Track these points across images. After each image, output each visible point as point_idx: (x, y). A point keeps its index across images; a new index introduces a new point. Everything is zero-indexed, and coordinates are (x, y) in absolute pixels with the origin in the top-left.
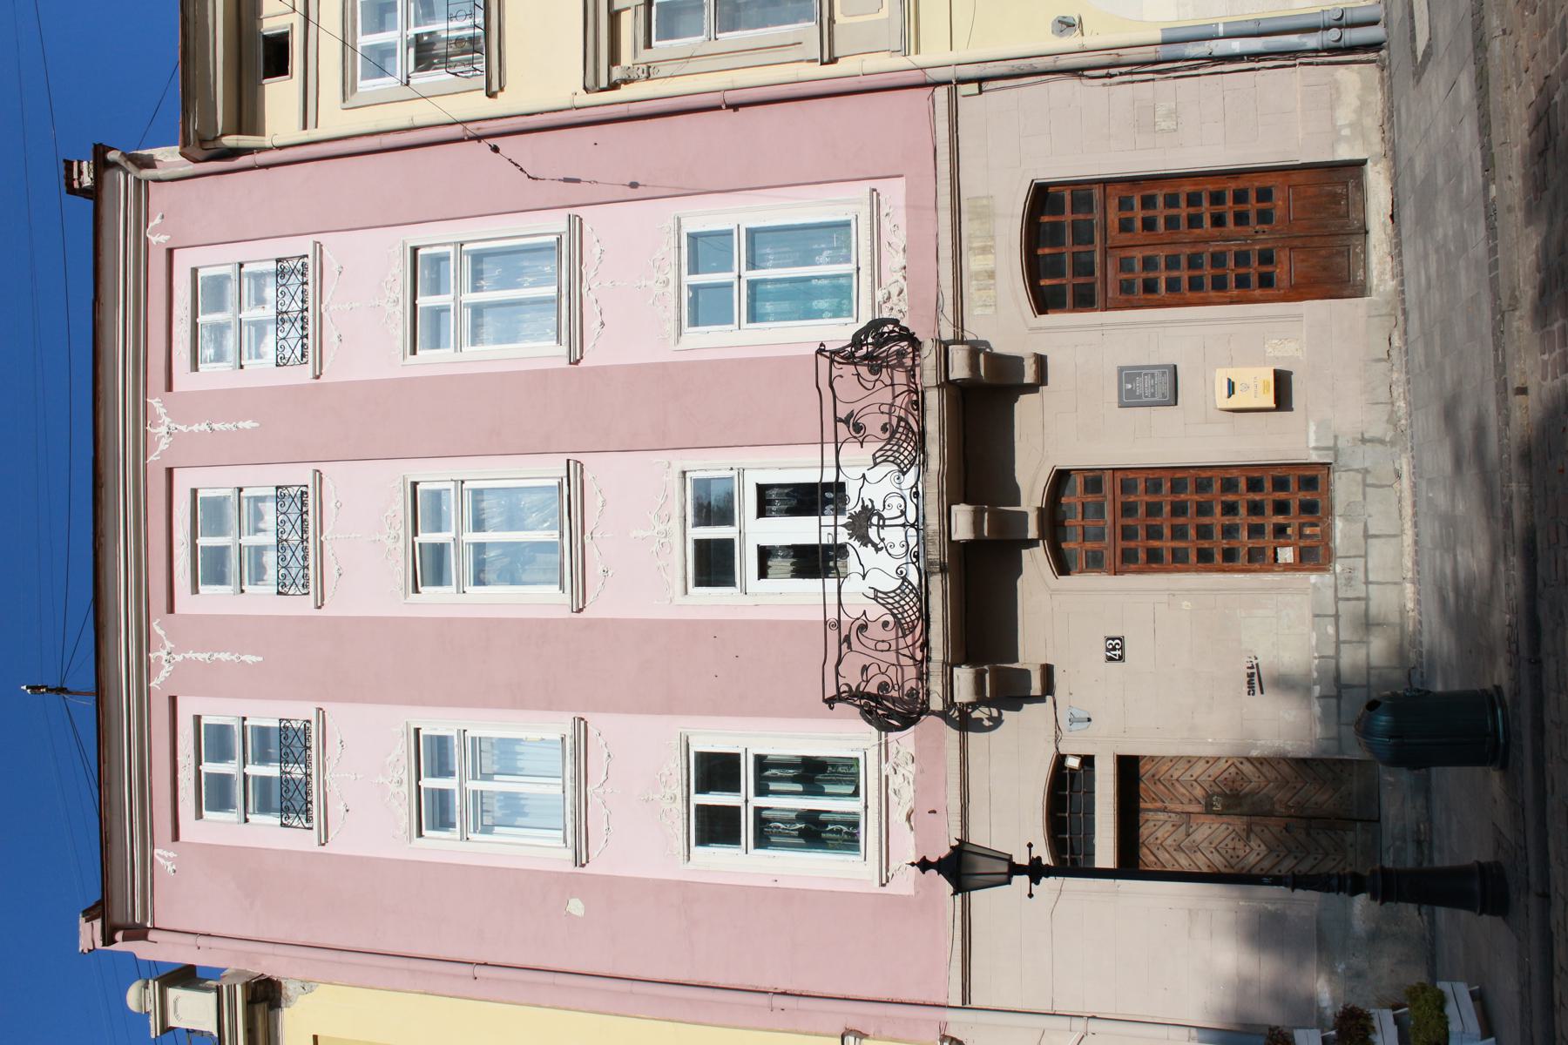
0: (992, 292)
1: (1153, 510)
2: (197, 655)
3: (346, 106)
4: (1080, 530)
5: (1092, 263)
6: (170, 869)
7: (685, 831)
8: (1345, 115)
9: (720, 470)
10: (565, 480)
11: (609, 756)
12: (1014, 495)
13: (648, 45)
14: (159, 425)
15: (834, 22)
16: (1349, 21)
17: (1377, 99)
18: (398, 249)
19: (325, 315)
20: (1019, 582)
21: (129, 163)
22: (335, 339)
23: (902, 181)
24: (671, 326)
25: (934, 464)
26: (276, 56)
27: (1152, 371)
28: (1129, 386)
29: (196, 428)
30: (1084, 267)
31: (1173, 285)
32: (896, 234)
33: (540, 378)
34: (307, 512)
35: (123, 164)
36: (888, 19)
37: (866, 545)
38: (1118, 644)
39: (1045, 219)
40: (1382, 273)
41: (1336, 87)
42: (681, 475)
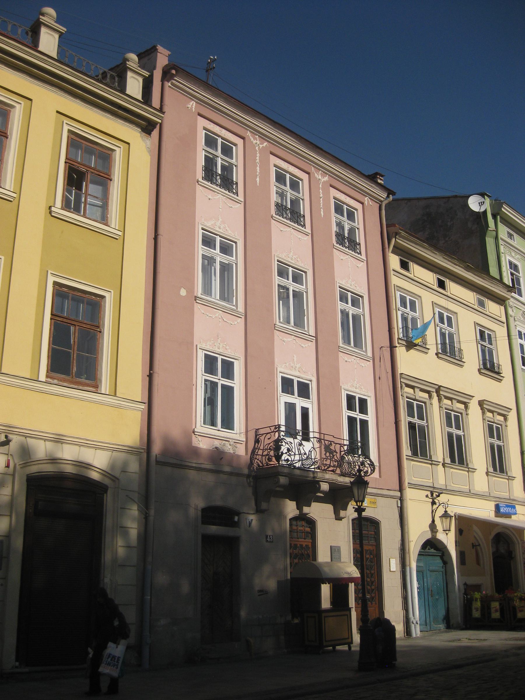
2: (258, 156)
6: (189, 106)
7: (210, 350)
11: (232, 324)
14: (321, 176)
21: (388, 202)
22: (342, 258)
26: (404, 265)
29: (321, 191)
35: (388, 200)
36: (412, 479)
38: (271, 540)
42: (311, 380)
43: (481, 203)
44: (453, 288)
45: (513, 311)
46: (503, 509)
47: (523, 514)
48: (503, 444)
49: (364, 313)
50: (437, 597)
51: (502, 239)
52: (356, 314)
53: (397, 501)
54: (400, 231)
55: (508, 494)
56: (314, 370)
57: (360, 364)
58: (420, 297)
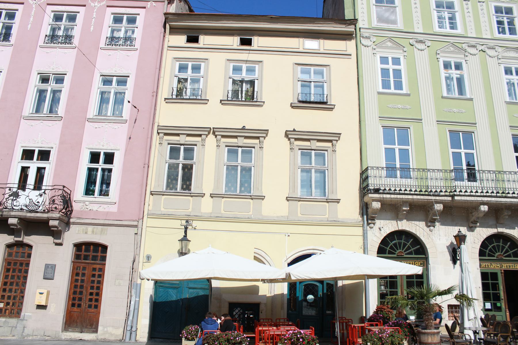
0: (82, 233)
1: (20, 271)
4: (18, 251)
5: (87, 260)
8: (110, 330)
12: (28, 234)
17: (112, 338)
19: (117, 51)
20: (6, 235)
24: (91, 146)
25: (29, 215)
26: (193, 39)
28: (50, 267)
29: (95, 14)
30: (86, 258)
31: (77, 280)
32: (103, 208)
33: (85, 110)
34: (65, 44)
37: (9, 196)
39: (100, 248)
40: (67, 336)
41: (118, 328)
44: (258, 41)
48: (327, 169)
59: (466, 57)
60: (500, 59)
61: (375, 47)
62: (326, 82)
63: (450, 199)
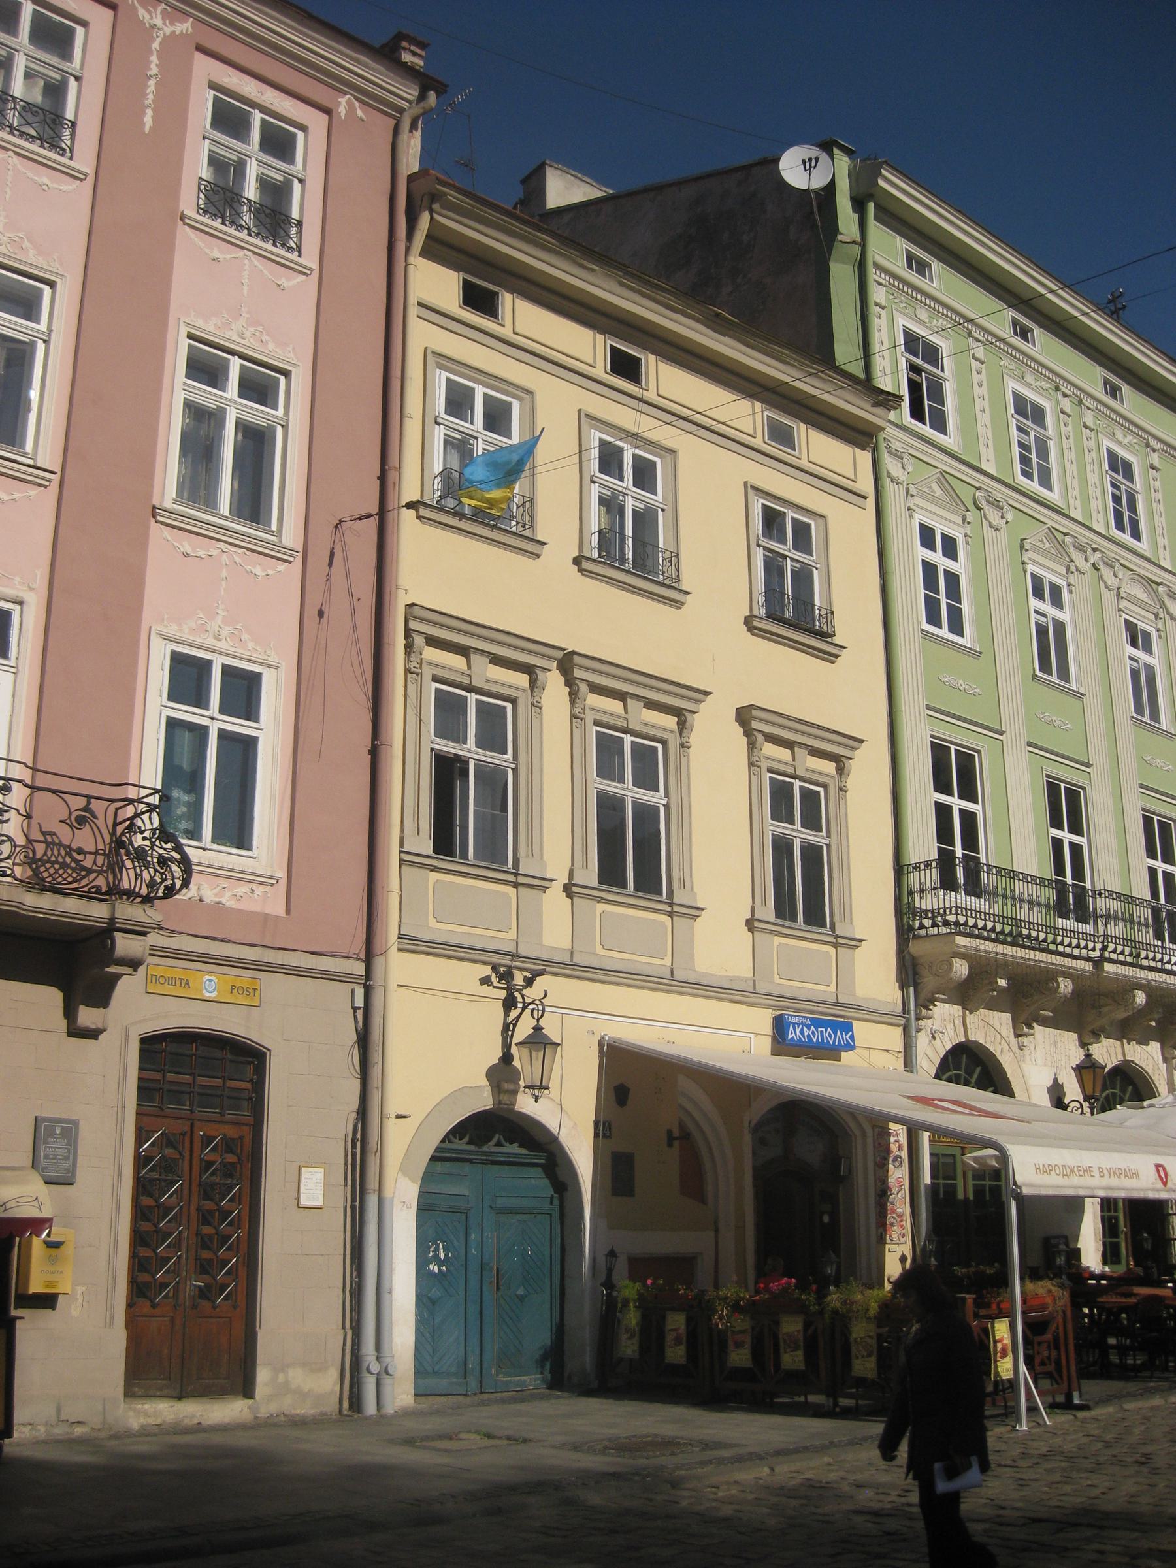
3: (429, 356)
8: (298, 1377)
9: (18, 646)
10: (31, 462)
13: (436, 679)
14: (163, 19)
15: (432, 871)
16: (382, 1382)
17: (305, 1409)
18: (291, 357)
19: (241, 253)
22: (216, 254)
23: (281, 912)
24: (172, 630)
27: (71, 1158)
28: (58, 1131)
29: (154, 59)
34: (42, 146)
35: (422, 104)
36: (428, 926)
40: (146, 1415)
42: (20, 600)
43: (810, 160)
45: (904, 469)
46: (798, 1031)
47: (887, 1051)
48: (827, 842)
49: (287, 421)
50: (521, 1292)
51: (877, 266)
52: (217, 406)
53: (353, 991)
54: (438, 187)
55: (833, 988)
56: (38, 573)
57: (248, 568)
58: (530, 392)
59: (1070, 574)
60: (1122, 598)
61: (913, 491)
62: (817, 569)
63: (1088, 966)
